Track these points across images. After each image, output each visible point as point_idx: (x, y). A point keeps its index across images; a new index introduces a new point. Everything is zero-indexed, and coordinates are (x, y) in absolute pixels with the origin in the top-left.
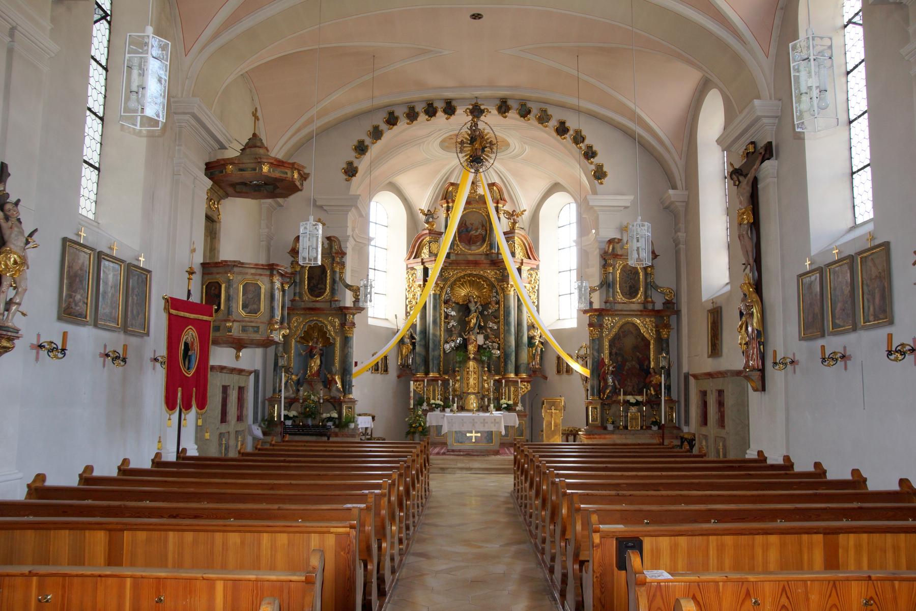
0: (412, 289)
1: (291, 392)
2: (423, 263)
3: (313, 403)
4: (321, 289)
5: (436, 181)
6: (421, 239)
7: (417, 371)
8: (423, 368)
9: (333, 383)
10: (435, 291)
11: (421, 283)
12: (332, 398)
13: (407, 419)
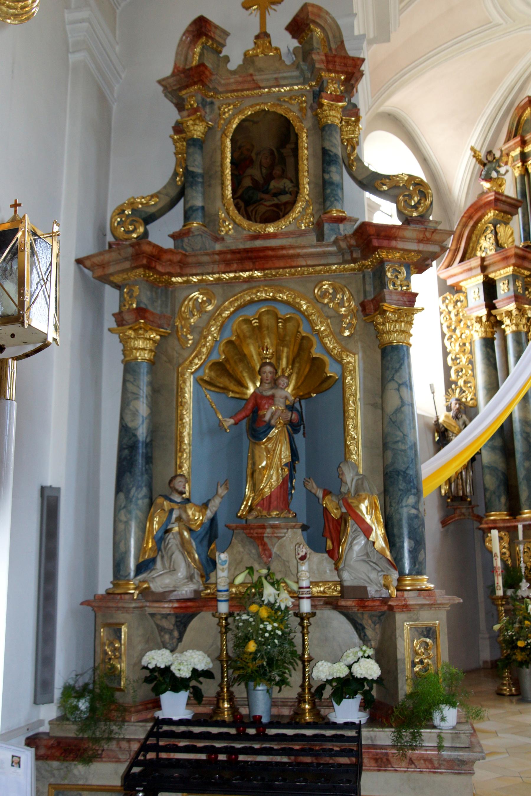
0: (458, 332)
1: (182, 573)
2: (484, 268)
3: (271, 619)
4: (283, 192)
5: (489, 110)
6: (475, 218)
7: (489, 508)
8: (503, 500)
9: (351, 526)
10: (517, 325)
11: (483, 312)
12: (345, 592)
13: (497, 627)
